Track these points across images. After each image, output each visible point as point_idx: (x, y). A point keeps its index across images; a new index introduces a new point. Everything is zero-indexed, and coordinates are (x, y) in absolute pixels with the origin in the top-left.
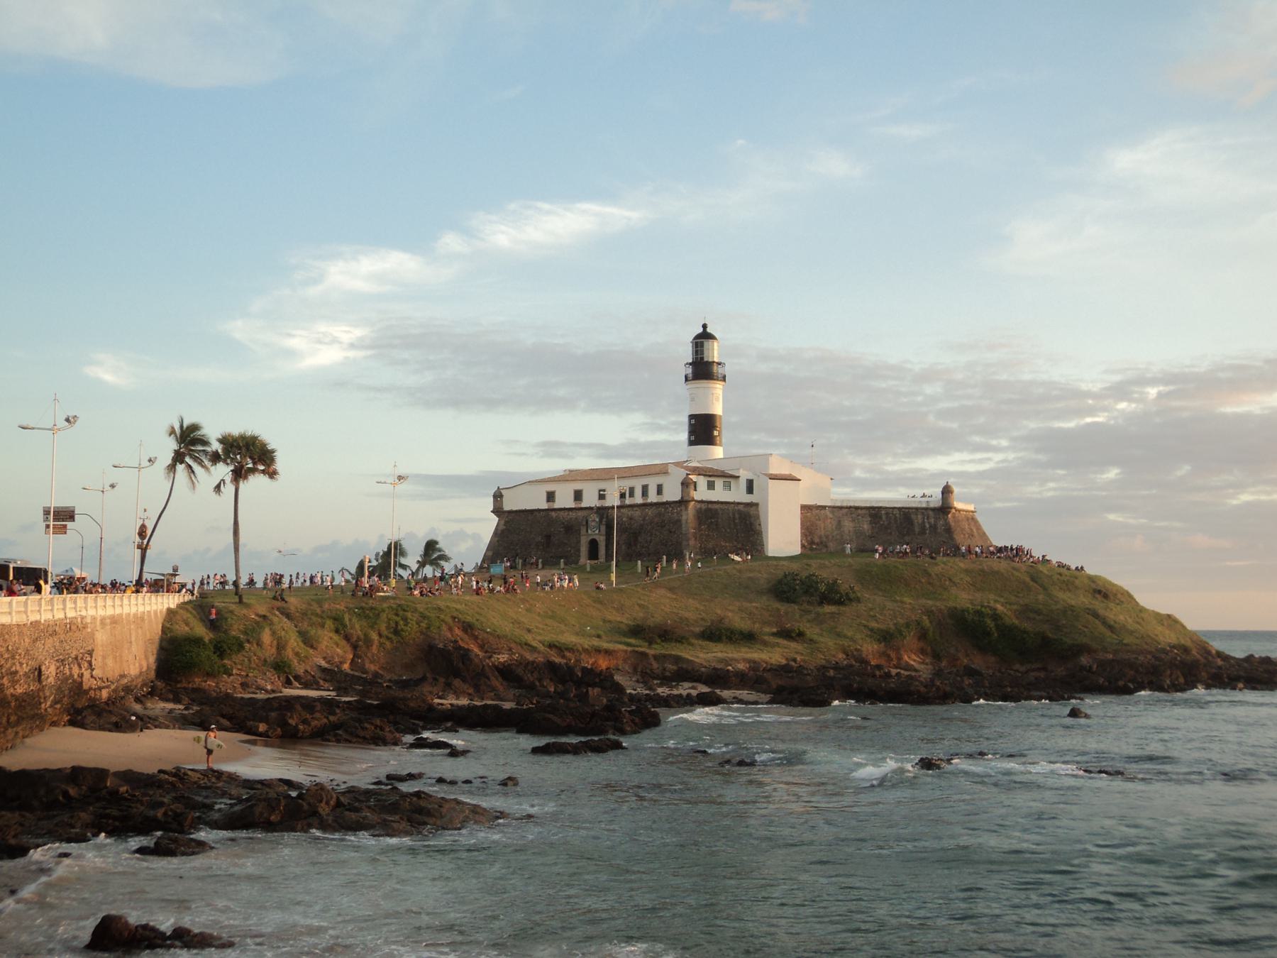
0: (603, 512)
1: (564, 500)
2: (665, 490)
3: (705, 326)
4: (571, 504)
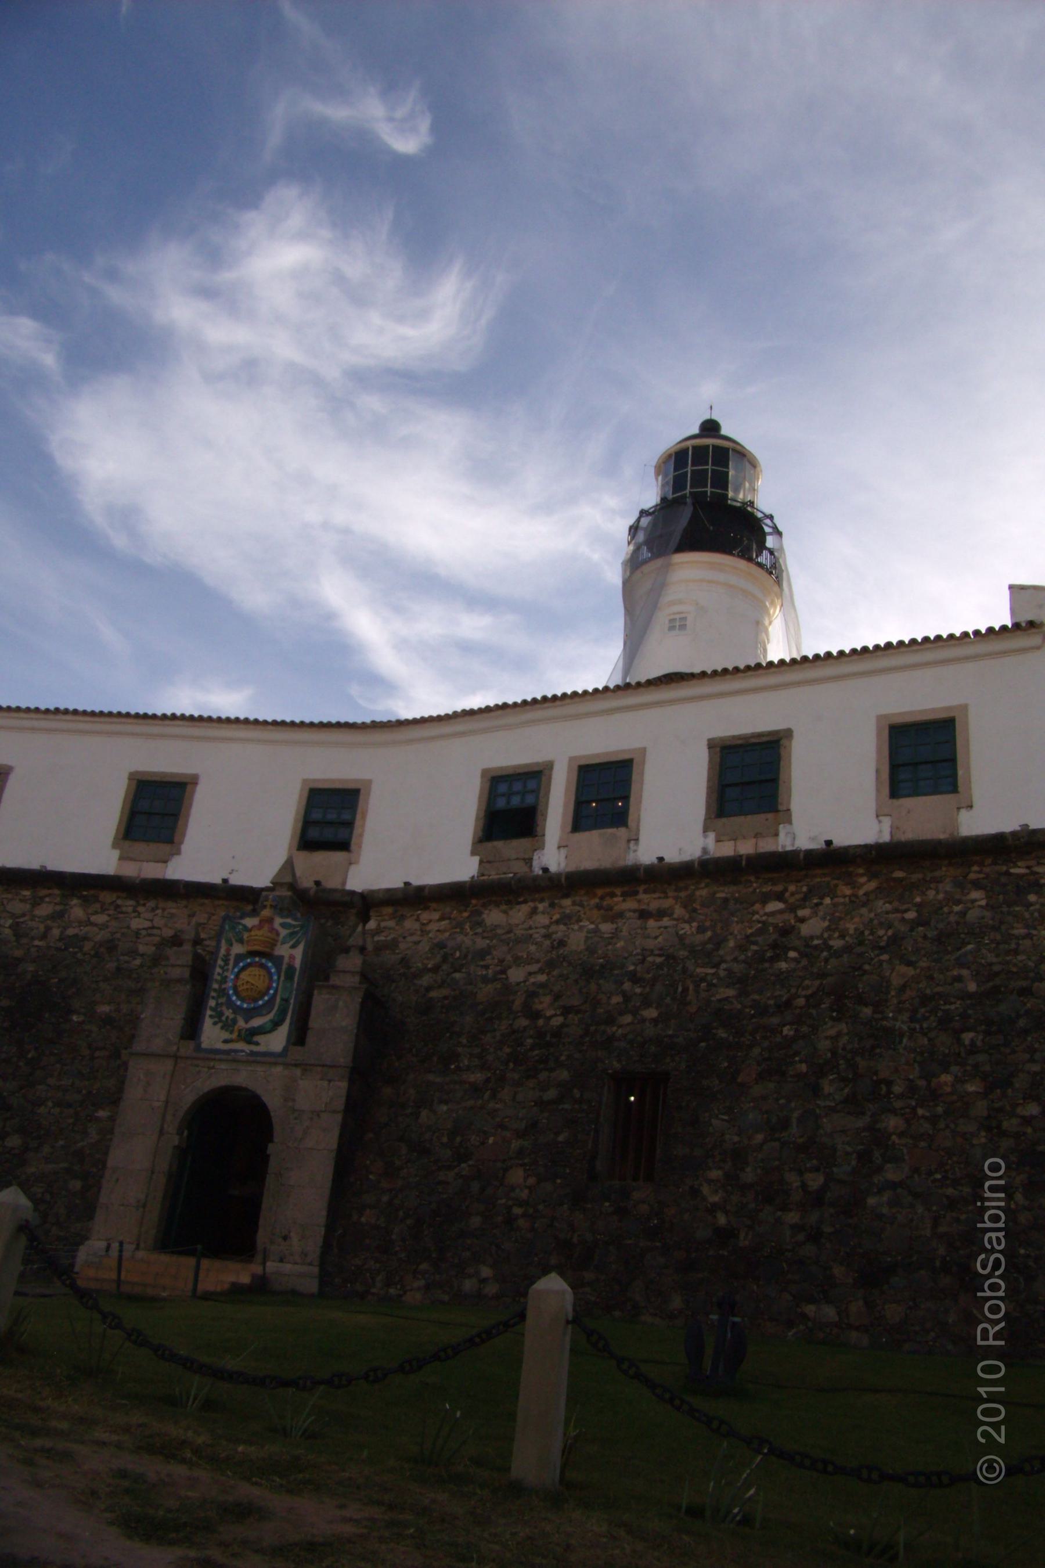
0: (325, 912)
2: (982, 757)
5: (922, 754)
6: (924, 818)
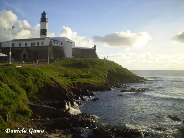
0: (26, 48)
1: (17, 45)
2: (44, 43)
3: (44, 11)
4: (18, 46)
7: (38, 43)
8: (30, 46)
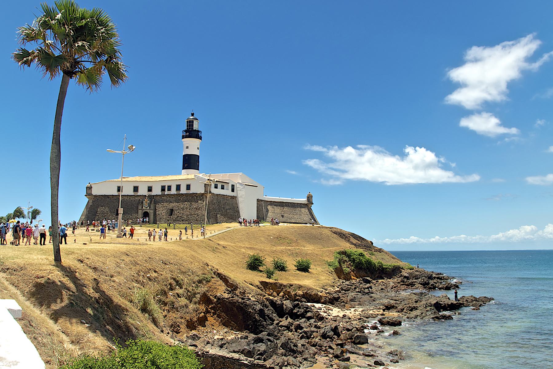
5: (188, 187)
6: (188, 192)
7: (178, 187)
8: (159, 192)
